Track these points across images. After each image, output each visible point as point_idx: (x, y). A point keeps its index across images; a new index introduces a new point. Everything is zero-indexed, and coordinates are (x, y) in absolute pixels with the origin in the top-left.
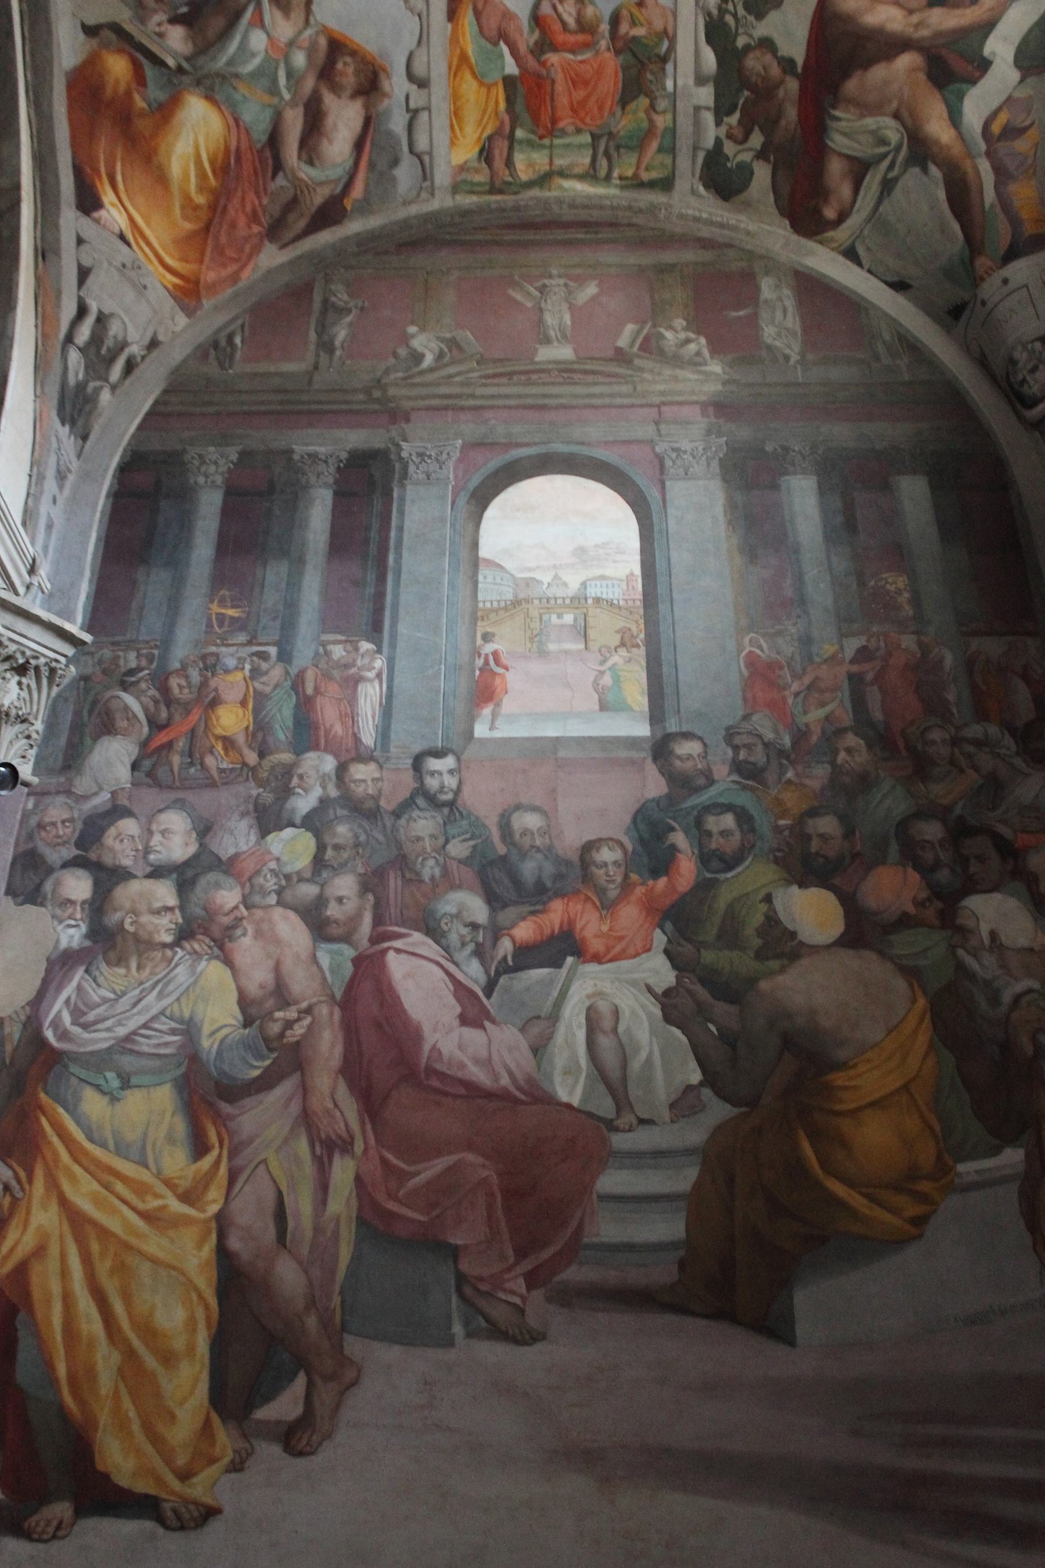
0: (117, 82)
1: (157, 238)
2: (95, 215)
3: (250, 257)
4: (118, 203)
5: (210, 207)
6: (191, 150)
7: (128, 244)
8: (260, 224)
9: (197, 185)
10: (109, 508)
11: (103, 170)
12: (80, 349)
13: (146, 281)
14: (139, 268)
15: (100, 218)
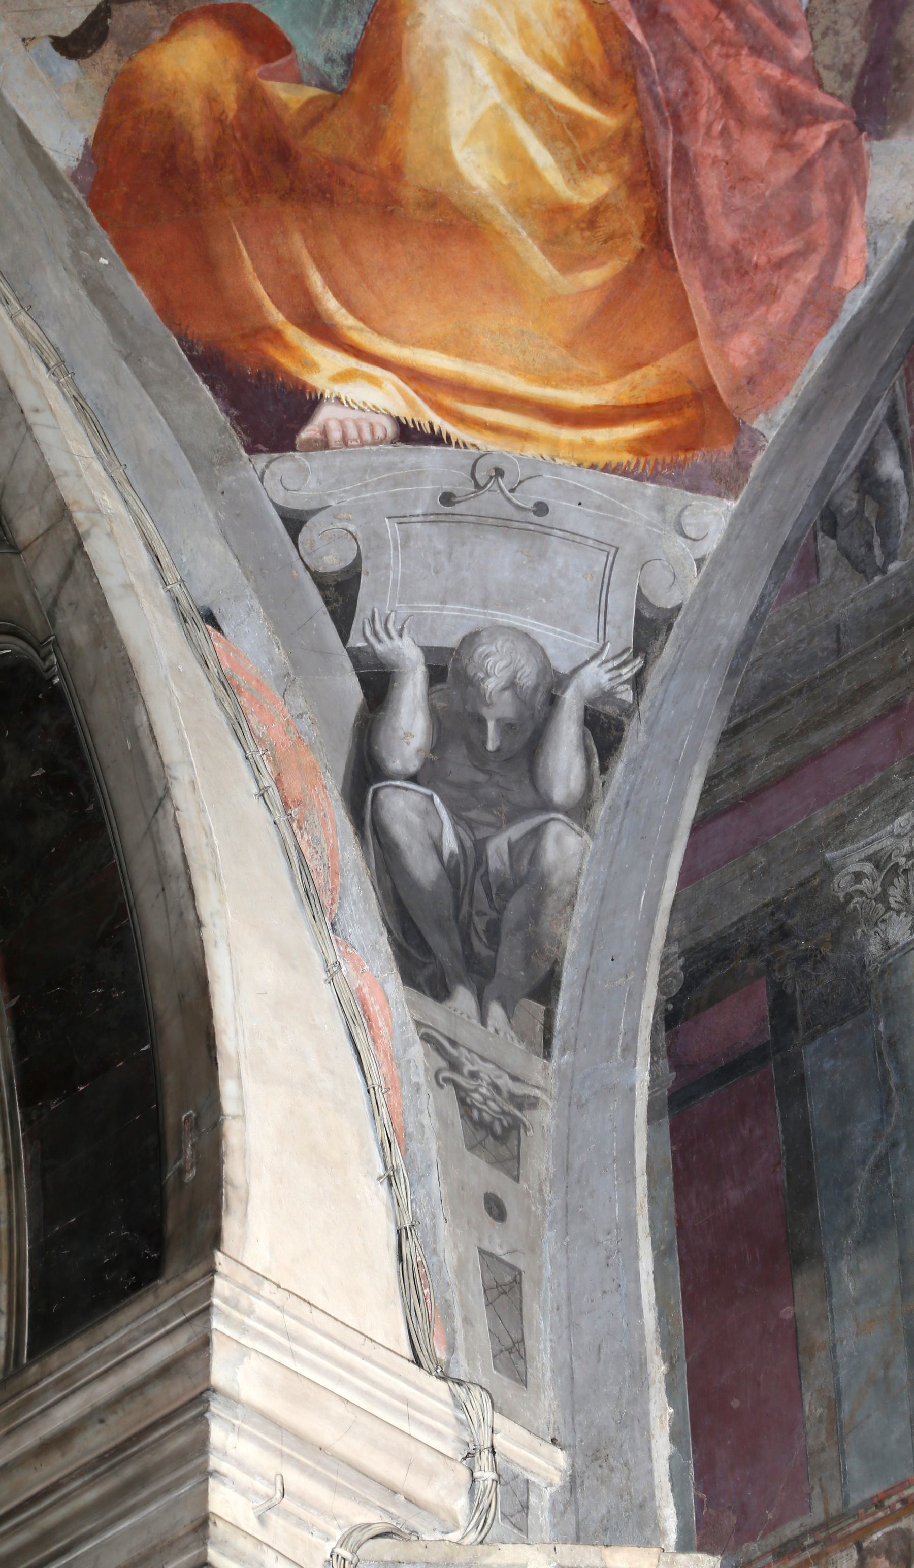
0: (211, 99)
1: (514, 370)
2: (308, 433)
3: (841, 218)
4: (352, 363)
5: (633, 186)
6: (495, 96)
7: (436, 439)
8: (817, 116)
9: (564, 166)
10: (666, 1150)
11: (277, 317)
12: (414, 778)
13: (528, 497)
14: (499, 472)
15: (325, 432)
